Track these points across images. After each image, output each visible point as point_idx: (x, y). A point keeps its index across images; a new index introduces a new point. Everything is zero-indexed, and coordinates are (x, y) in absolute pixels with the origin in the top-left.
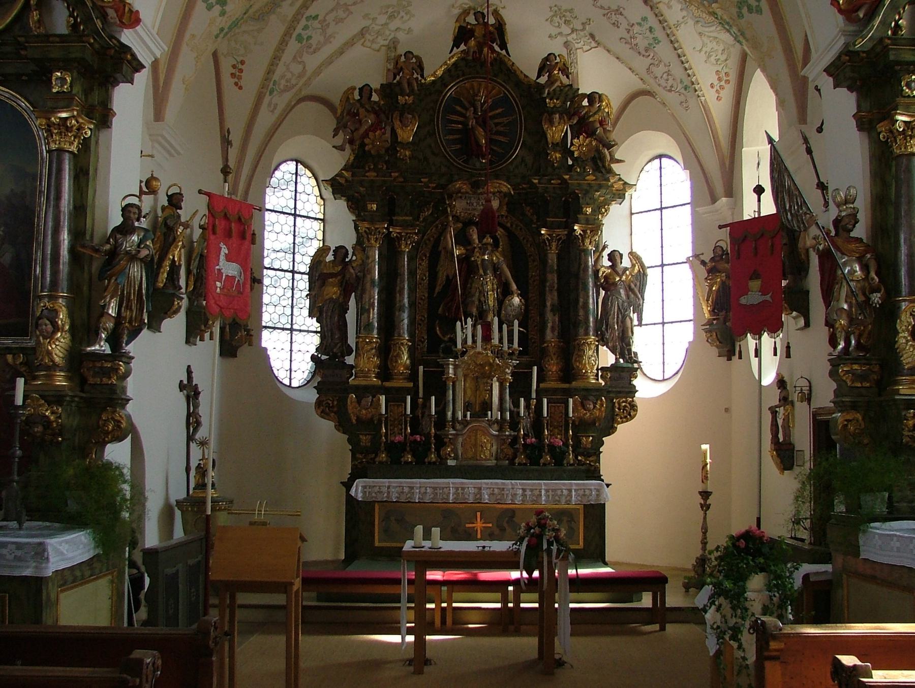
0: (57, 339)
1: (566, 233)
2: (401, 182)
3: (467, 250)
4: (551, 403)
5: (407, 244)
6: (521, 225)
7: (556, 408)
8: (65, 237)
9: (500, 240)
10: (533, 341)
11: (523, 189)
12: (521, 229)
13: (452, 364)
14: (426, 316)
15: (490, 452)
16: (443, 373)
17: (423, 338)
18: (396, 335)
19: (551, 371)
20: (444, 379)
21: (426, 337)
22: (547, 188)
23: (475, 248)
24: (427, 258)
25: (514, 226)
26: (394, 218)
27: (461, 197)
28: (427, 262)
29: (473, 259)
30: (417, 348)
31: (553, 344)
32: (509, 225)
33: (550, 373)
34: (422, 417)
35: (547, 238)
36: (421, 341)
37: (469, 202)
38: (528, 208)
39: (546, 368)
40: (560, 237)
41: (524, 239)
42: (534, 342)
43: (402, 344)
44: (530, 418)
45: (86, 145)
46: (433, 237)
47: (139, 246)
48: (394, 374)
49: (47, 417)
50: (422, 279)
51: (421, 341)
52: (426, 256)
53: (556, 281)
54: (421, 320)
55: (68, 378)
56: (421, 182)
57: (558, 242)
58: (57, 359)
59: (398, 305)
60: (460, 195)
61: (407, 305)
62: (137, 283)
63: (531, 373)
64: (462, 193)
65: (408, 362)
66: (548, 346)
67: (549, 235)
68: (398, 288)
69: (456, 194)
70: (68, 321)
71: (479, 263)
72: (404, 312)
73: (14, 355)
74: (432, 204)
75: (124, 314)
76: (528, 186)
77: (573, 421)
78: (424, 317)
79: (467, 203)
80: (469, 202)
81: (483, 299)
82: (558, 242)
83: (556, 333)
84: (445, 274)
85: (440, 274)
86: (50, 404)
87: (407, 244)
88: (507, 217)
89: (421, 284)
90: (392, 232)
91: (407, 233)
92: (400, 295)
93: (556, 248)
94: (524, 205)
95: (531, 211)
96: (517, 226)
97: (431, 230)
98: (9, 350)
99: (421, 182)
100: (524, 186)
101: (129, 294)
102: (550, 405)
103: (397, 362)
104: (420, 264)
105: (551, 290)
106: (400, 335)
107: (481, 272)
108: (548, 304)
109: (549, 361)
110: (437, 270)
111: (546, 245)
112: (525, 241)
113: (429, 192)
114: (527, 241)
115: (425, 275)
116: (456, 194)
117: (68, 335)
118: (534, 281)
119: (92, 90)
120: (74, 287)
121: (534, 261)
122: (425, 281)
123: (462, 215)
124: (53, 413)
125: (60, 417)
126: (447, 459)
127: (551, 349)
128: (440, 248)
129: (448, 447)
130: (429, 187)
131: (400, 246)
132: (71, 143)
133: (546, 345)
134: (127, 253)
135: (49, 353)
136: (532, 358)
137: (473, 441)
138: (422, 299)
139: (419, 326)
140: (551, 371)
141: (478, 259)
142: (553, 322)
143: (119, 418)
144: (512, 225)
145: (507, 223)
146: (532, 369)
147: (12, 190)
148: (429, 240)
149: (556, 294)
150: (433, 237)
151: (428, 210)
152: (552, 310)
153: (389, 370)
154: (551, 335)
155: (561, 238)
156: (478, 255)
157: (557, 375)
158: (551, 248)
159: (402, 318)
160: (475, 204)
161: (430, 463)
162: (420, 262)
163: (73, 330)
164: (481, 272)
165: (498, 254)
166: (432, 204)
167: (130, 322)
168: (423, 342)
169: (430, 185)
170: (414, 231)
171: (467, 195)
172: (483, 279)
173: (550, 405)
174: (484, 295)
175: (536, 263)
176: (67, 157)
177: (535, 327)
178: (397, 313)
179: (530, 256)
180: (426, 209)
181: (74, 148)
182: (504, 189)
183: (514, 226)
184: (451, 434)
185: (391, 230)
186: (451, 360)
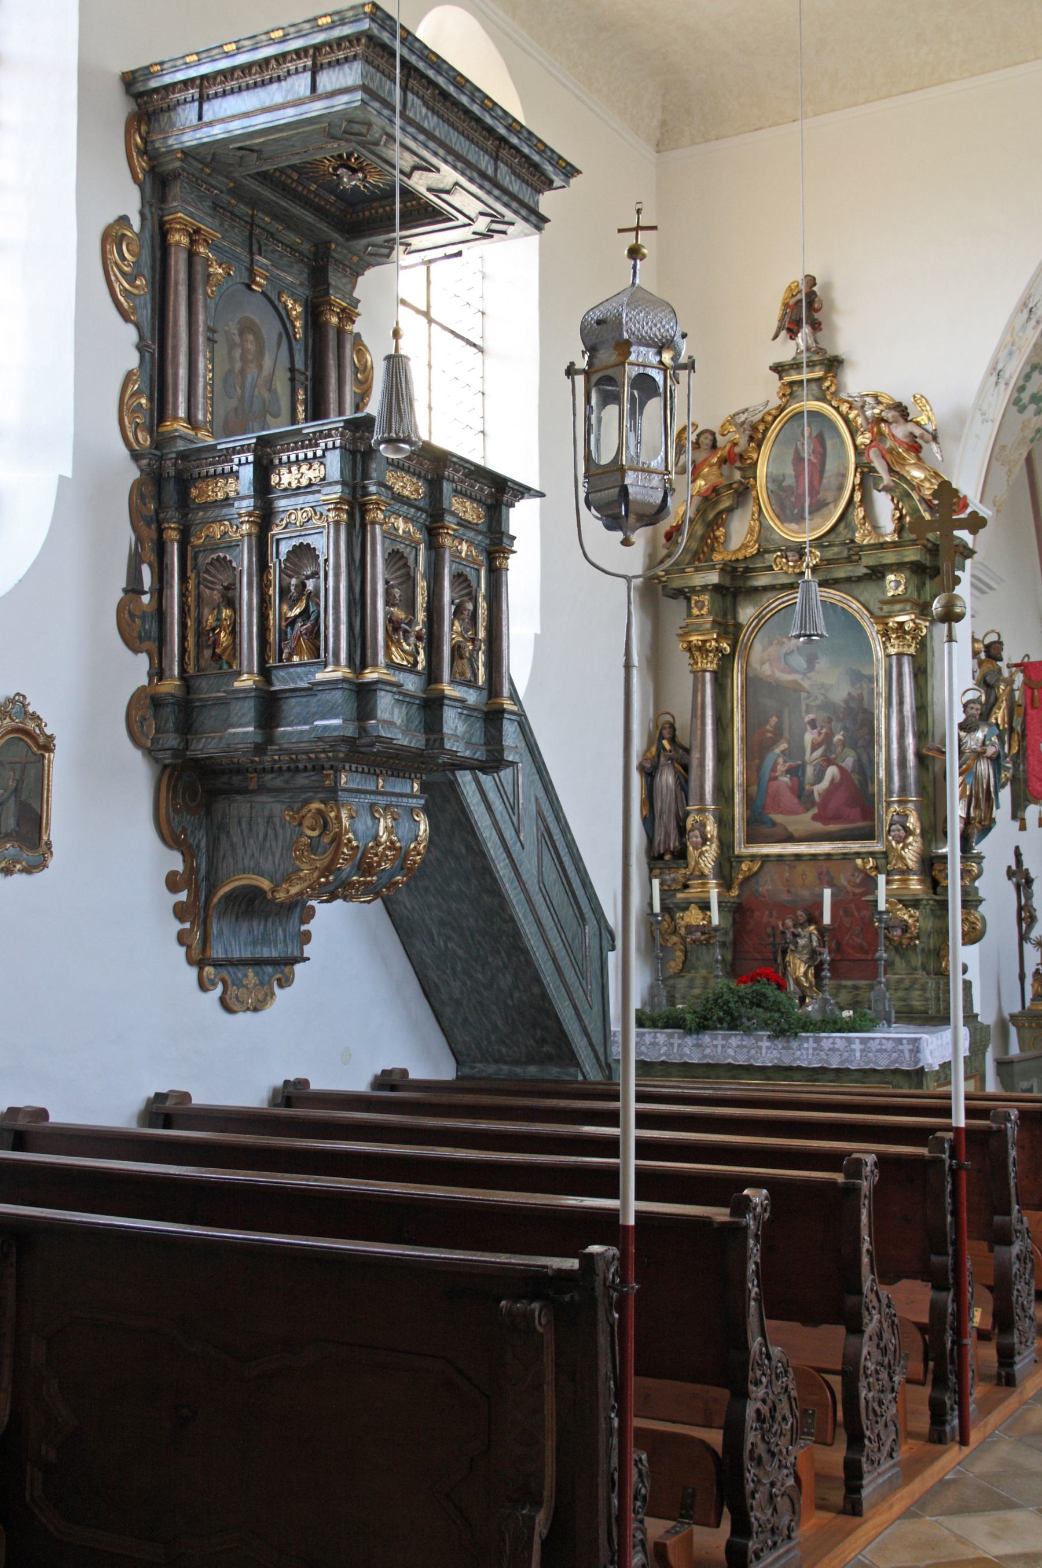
0: (910, 844)
8: (910, 741)
45: (923, 645)
47: (984, 744)
49: (905, 921)
55: (921, 882)
58: (910, 864)
62: (985, 781)
70: (918, 824)
73: (863, 859)
75: (972, 815)
86: (906, 906)
98: (858, 854)
101: (977, 793)
117: (919, 839)
119: (924, 584)
120: (922, 790)
124: (910, 916)
125: (917, 921)
132: (909, 646)
134: (974, 751)
135: (902, 858)
143: (974, 920)
147: (849, 694)
163: (923, 834)
167: (980, 822)
176: (906, 660)
181: (912, 650)
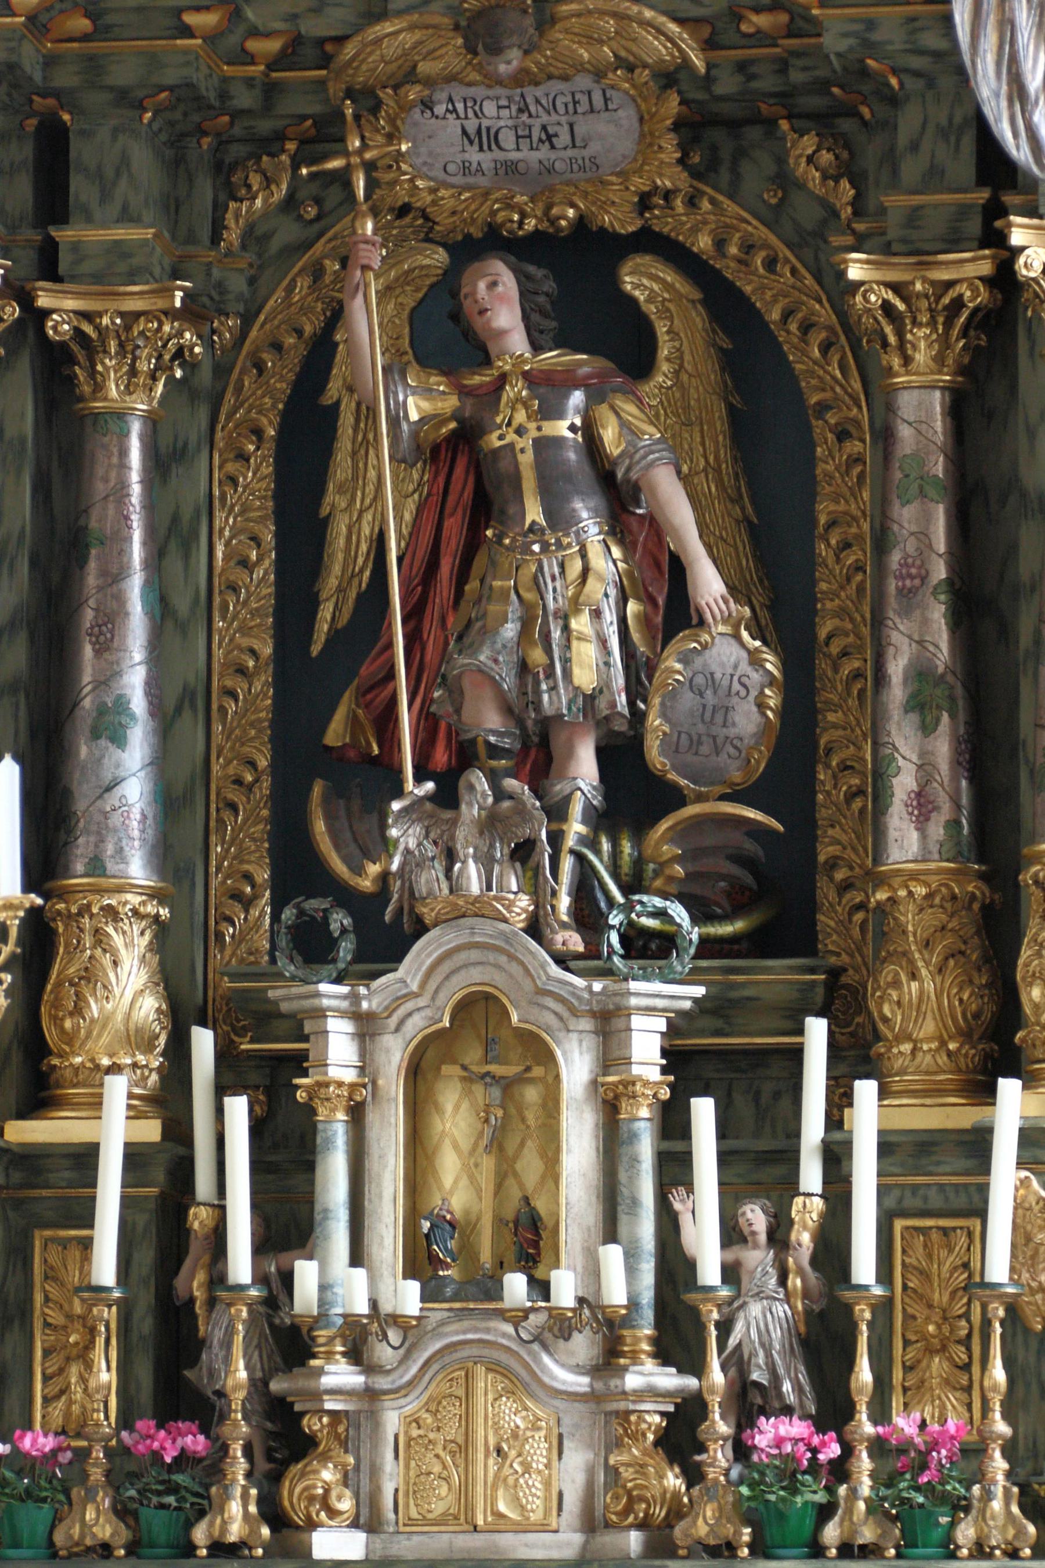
1: (985, 268)
2: (85, 38)
3: (464, 392)
4: (904, 1214)
5: (133, 372)
6: (773, 240)
7: (935, 1236)
9: (661, 329)
10: (840, 875)
11: (760, 38)
12: (771, 264)
13: (343, 1014)
14: (263, 763)
15: (547, 1484)
16: (299, 1063)
17: (248, 877)
18: (79, 867)
19: (909, 1038)
20: (301, 1096)
21: (263, 875)
22: (871, 24)
23: (503, 379)
24: (269, 448)
25: (733, 250)
26: (64, 235)
27: (427, 105)
28: (267, 469)
29: (494, 440)
30: (220, 936)
31: (920, 891)
32: (703, 243)
33: (906, 1047)
34: (212, 1302)
35: (887, 307)
36: (236, 896)
37: (471, 129)
38: (808, 143)
39: (885, 1020)
40: (952, 294)
41: (787, 315)
42: (845, 887)
43: (112, 913)
44: (788, 1299)
46: (299, 332)
48: (68, 1073)
50: (244, 563)
51: (236, 896)
52: (258, 433)
53: (941, 544)
54: (239, 782)
56: (187, 32)
57: (949, 324)
59: (87, 703)
60: (413, 93)
61: (138, 703)
63: (796, 1055)
64: (429, 82)
65: (149, 1007)
66: (893, 900)
67: (888, 285)
68: (88, 616)
69: (396, 88)
71: (526, 459)
72: (119, 740)
74: (291, 146)
76: (783, 18)
77: (1013, 1310)
78: (252, 764)
79: (464, 132)
80: (471, 129)
81: (537, 656)
82: (949, 324)
83: (937, 830)
84: (366, 530)
85: (340, 527)
87: (133, 372)
88: (692, 202)
89: (234, 588)
90: (46, 313)
91: (131, 318)
92: (98, 653)
93: (940, 360)
94: (784, 125)
95: (826, 157)
96: (748, 248)
97: (290, 289)
99: (187, 32)
100: (762, 21)
102: (899, 1224)
103: (78, 1011)
104: (233, 481)
105: (913, 591)
106: (97, 866)
107: (534, 513)
108: (897, 668)
109: (896, 984)
110: (324, 511)
111: (885, 344)
112: (793, 327)
113: (249, 82)
114: (806, 328)
115: (255, 540)
116: (396, 88)
118: (846, 545)
121: (842, 435)
122: (259, 573)
123: (449, 204)
126: (312, 1525)
127: (909, 918)
128: (334, 389)
129: (325, 1458)
130: (251, 59)
131: (99, 388)
133: (881, 896)
136: (812, 971)
137: (453, 1431)
138: (241, 671)
139: (227, 815)
140: (909, 1038)
141: (521, 443)
142: (925, 768)
144: (720, 244)
145: (695, 230)
146: (800, 1031)
148: (277, 347)
149: (938, 614)
150: (299, 332)
151: (268, 181)
152: (917, 704)
153: (50, 1053)
154: (914, 836)
155: (958, 304)
156: (520, 417)
157: (943, 1059)
158: (907, 360)
159: (107, 776)
160: (507, 139)
161: (220, 1549)
162: (231, 467)
164: (534, 513)
165: (629, 409)
166: (291, 146)
168: (247, 903)
169: (252, 45)
170: (161, 304)
171: (459, 92)
172: (545, 547)
173: (899, 1224)
174: (546, 637)
175: (854, 447)
177: (850, 797)
178: (84, 751)
179: (823, 408)
180: (255, 180)
182: (657, 49)
183: (733, 250)
184: (334, 1392)
185: (43, 301)
186: (324, 987)
